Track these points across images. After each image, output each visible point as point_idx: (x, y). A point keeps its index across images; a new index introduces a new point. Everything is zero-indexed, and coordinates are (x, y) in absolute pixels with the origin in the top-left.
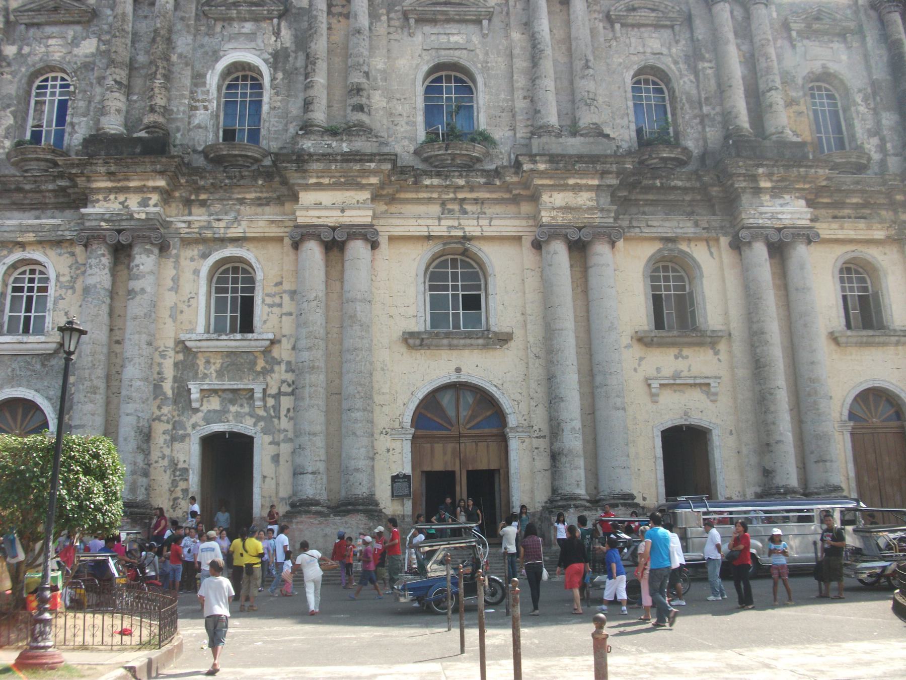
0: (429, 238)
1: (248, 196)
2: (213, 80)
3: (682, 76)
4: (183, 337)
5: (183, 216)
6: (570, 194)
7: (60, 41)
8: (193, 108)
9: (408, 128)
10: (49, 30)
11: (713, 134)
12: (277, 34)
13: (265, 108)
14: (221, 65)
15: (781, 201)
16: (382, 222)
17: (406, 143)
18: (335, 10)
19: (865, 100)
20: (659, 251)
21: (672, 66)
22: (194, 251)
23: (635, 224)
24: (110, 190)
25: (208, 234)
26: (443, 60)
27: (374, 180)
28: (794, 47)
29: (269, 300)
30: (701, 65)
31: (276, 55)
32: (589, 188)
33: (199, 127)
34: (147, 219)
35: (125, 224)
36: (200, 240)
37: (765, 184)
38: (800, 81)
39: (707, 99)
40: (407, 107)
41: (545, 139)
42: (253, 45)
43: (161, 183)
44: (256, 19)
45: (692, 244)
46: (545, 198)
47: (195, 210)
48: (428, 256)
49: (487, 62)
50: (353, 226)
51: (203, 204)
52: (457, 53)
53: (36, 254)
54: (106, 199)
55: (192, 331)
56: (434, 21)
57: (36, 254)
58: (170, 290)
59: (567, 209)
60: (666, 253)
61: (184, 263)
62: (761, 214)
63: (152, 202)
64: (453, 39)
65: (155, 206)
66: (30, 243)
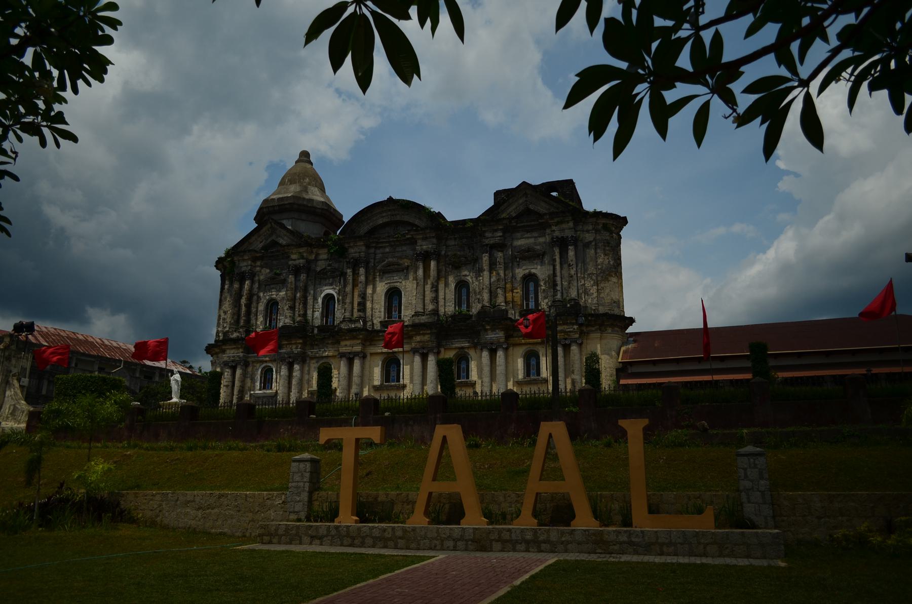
0: (382, 353)
1: (330, 342)
2: (320, 300)
3: (473, 283)
4: (309, 389)
5: (311, 349)
6: (422, 336)
7: (275, 290)
8: (313, 311)
9: (379, 313)
10: (272, 286)
11: (479, 306)
12: (340, 283)
13: (336, 310)
14: (322, 295)
15: (495, 333)
16: (367, 349)
17: (378, 319)
18: (357, 272)
19: (545, 284)
20: (457, 353)
21: (471, 281)
22: (314, 361)
23: (448, 343)
24: (287, 344)
25: (317, 355)
26: (391, 286)
27: (361, 337)
28: (518, 265)
29: (335, 376)
30: (479, 279)
31: (339, 290)
32: (428, 334)
33: (316, 318)
34: (298, 353)
35: (292, 355)
36: (315, 358)
37: (488, 327)
38: (518, 279)
39: (479, 292)
40: (379, 306)
41: (414, 318)
42: (332, 287)
43: (301, 341)
44: (333, 278)
45: (469, 349)
46: (414, 338)
47: (315, 347)
48: (383, 358)
49: (405, 286)
50: (355, 352)
51: (317, 345)
52: (396, 284)
53: (270, 365)
54: (286, 347)
55: (312, 387)
56: (388, 272)
57: (270, 365)
58: (306, 374)
59: (418, 342)
60: (460, 353)
61: (311, 365)
62: (486, 338)
63: (299, 347)
64: (395, 278)
65: (300, 348)
66: (268, 361)
